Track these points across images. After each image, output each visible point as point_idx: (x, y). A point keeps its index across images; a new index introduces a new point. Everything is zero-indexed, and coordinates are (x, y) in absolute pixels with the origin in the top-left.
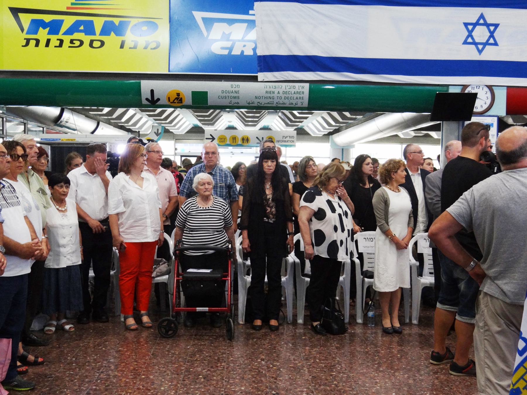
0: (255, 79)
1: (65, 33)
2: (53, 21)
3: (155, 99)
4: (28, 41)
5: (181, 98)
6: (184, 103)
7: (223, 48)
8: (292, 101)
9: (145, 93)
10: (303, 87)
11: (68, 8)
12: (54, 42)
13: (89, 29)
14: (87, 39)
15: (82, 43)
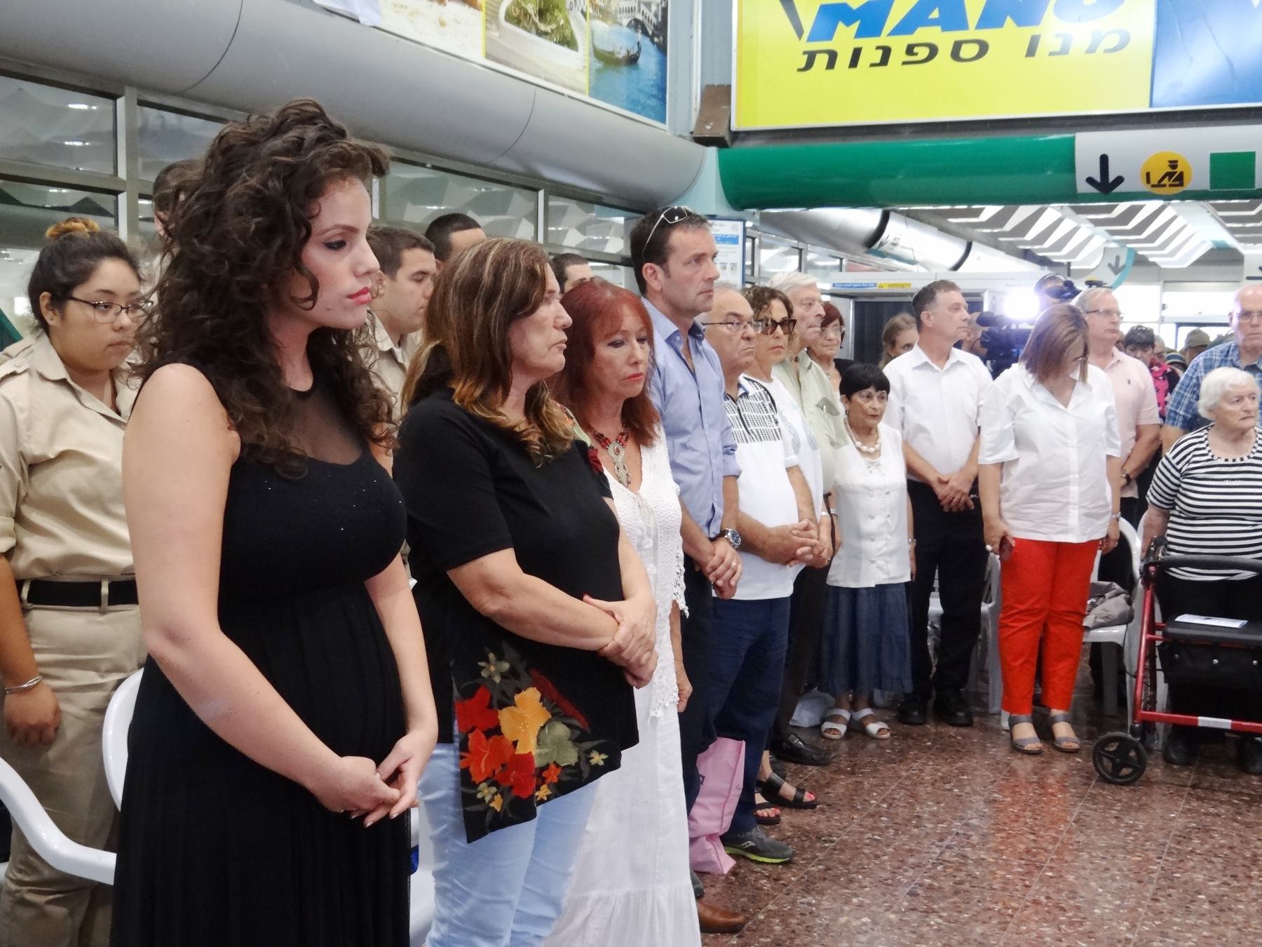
1: (894, 32)
3: (1112, 178)
4: (811, 57)
5: (1181, 174)
6: (1190, 185)
9: (1087, 167)
12: (871, 53)
14: (944, 41)
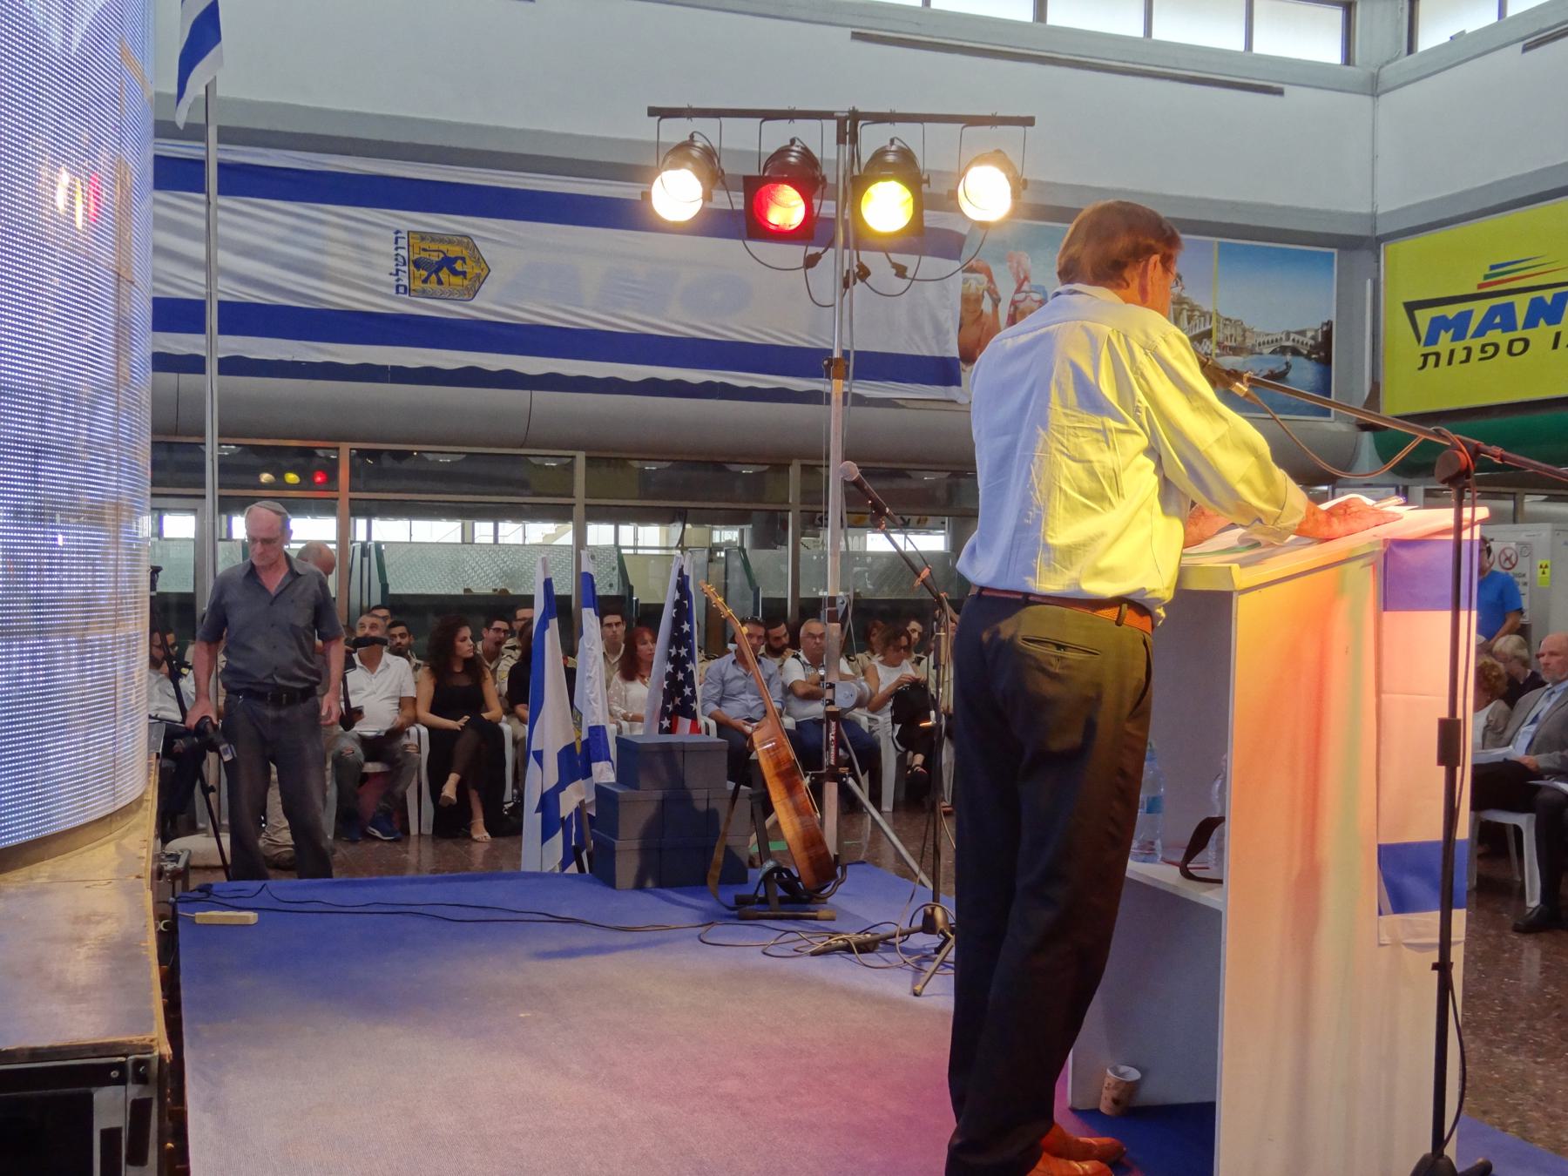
2: (1460, 315)
4: (1426, 356)
11: (1480, 286)
12: (1460, 355)
13: (1504, 317)
15: (1497, 347)
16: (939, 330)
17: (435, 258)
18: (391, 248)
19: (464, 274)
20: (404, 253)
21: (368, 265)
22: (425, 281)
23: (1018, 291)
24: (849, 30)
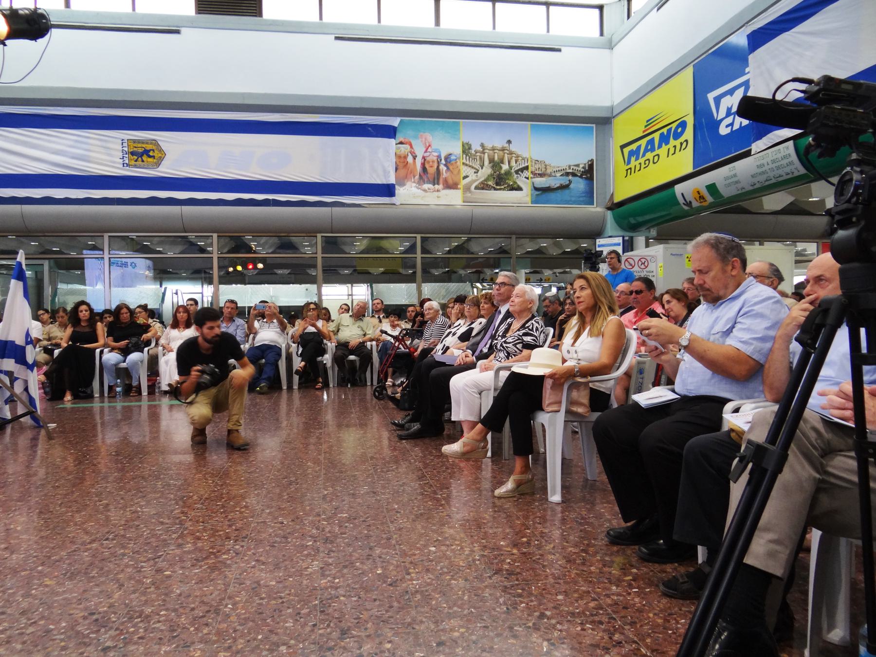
0: (748, 154)
7: (727, 126)
8: (780, 172)
10: (787, 148)
11: (644, 131)
16: (386, 173)
17: (140, 150)
18: (120, 147)
19: (154, 157)
20: (126, 149)
21: (109, 155)
22: (136, 161)
23: (426, 151)
24: (333, 36)
